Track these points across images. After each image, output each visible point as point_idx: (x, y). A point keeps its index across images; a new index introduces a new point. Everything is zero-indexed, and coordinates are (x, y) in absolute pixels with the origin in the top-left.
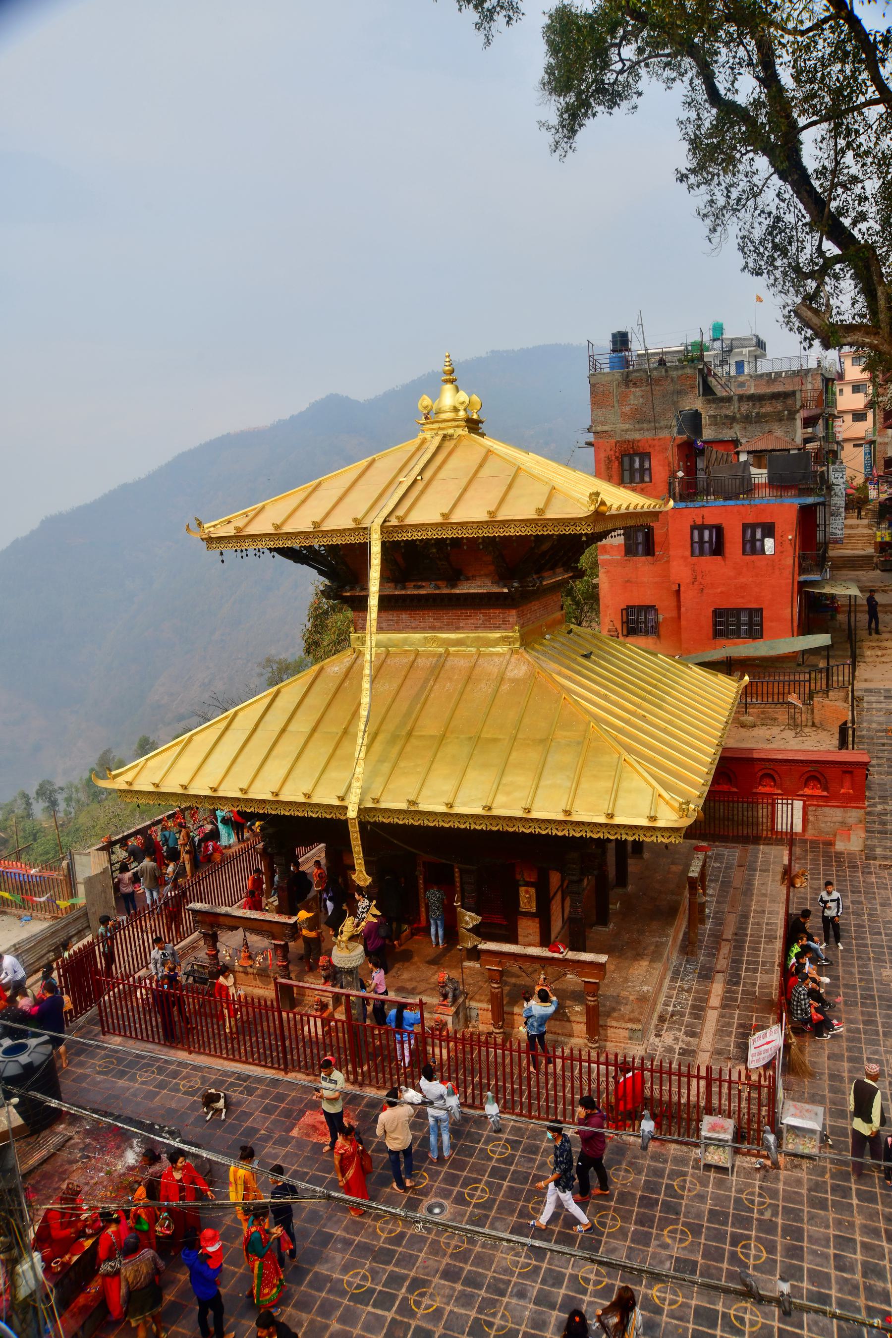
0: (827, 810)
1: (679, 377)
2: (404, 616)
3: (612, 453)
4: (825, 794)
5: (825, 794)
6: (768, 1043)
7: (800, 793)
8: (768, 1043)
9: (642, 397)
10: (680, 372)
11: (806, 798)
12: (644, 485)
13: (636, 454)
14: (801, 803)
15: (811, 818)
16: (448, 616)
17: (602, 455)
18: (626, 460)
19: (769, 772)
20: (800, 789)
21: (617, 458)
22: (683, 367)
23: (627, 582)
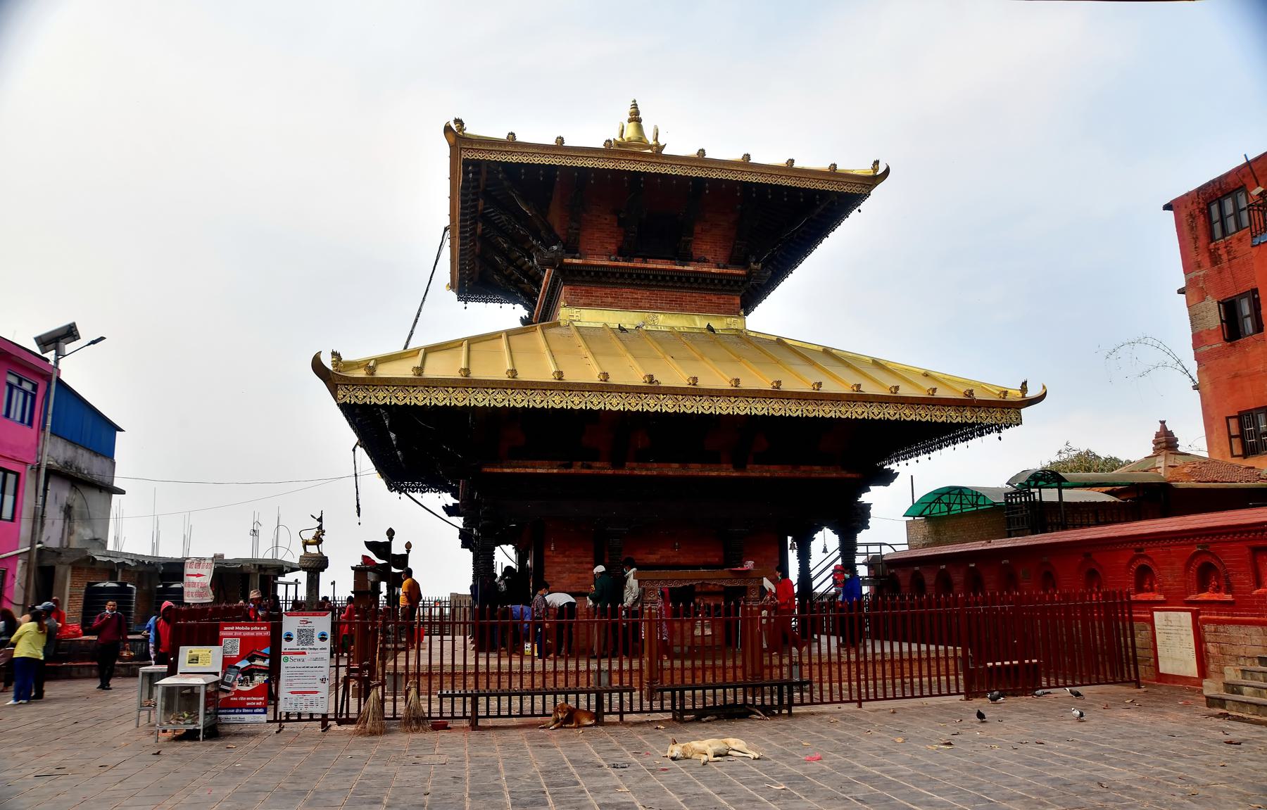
0: (1232, 630)
3: (1195, 206)
4: (1229, 597)
5: (1229, 597)
6: (199, 575)
7: (1192, 598)
8: (199, 575)
11: (1197, 610)
12: (1242, 232)
14: (1186, 618)
15: (1211, 648)
17: (1184, 215)
18: (1215, 209)
19: (1146, 562)
20: (1187, 593)
21: (1201, 211)
23: (1235, 376)
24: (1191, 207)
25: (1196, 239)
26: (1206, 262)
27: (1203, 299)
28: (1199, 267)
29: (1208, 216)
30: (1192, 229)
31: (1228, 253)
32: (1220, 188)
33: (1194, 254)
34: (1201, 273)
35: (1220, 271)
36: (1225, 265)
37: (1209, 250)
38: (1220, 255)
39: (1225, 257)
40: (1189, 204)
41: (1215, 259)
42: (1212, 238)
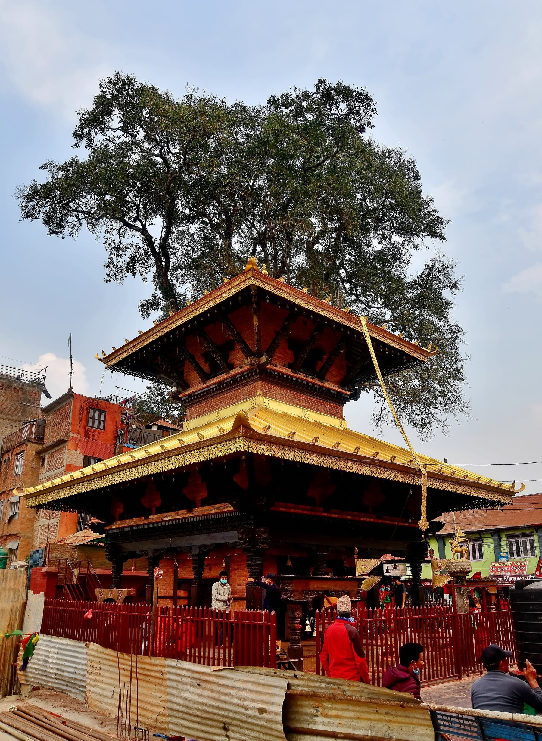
1: (30, 392)
2: (290, 394)
9: (4, 396)
10: (31, 389)
13: (98, 410)
16: (314, 400)
22: (34, 386)
24: (82, 404)
25: (81, 420)
26: (82, 433)
27: (76, 450)
28: (79, 433)
29: (88, 413)
30: (80, 414)
31: (93, 436)
32: (97, 405)
33: (78, 426)
34: (79, 437)
35: (87, 441)
36: (90, 440)
37: (85, 429)
38: (89, 435)
39: (91, 436)
40: (82, 401)
41: (87, 435)
42: (87, 424)
